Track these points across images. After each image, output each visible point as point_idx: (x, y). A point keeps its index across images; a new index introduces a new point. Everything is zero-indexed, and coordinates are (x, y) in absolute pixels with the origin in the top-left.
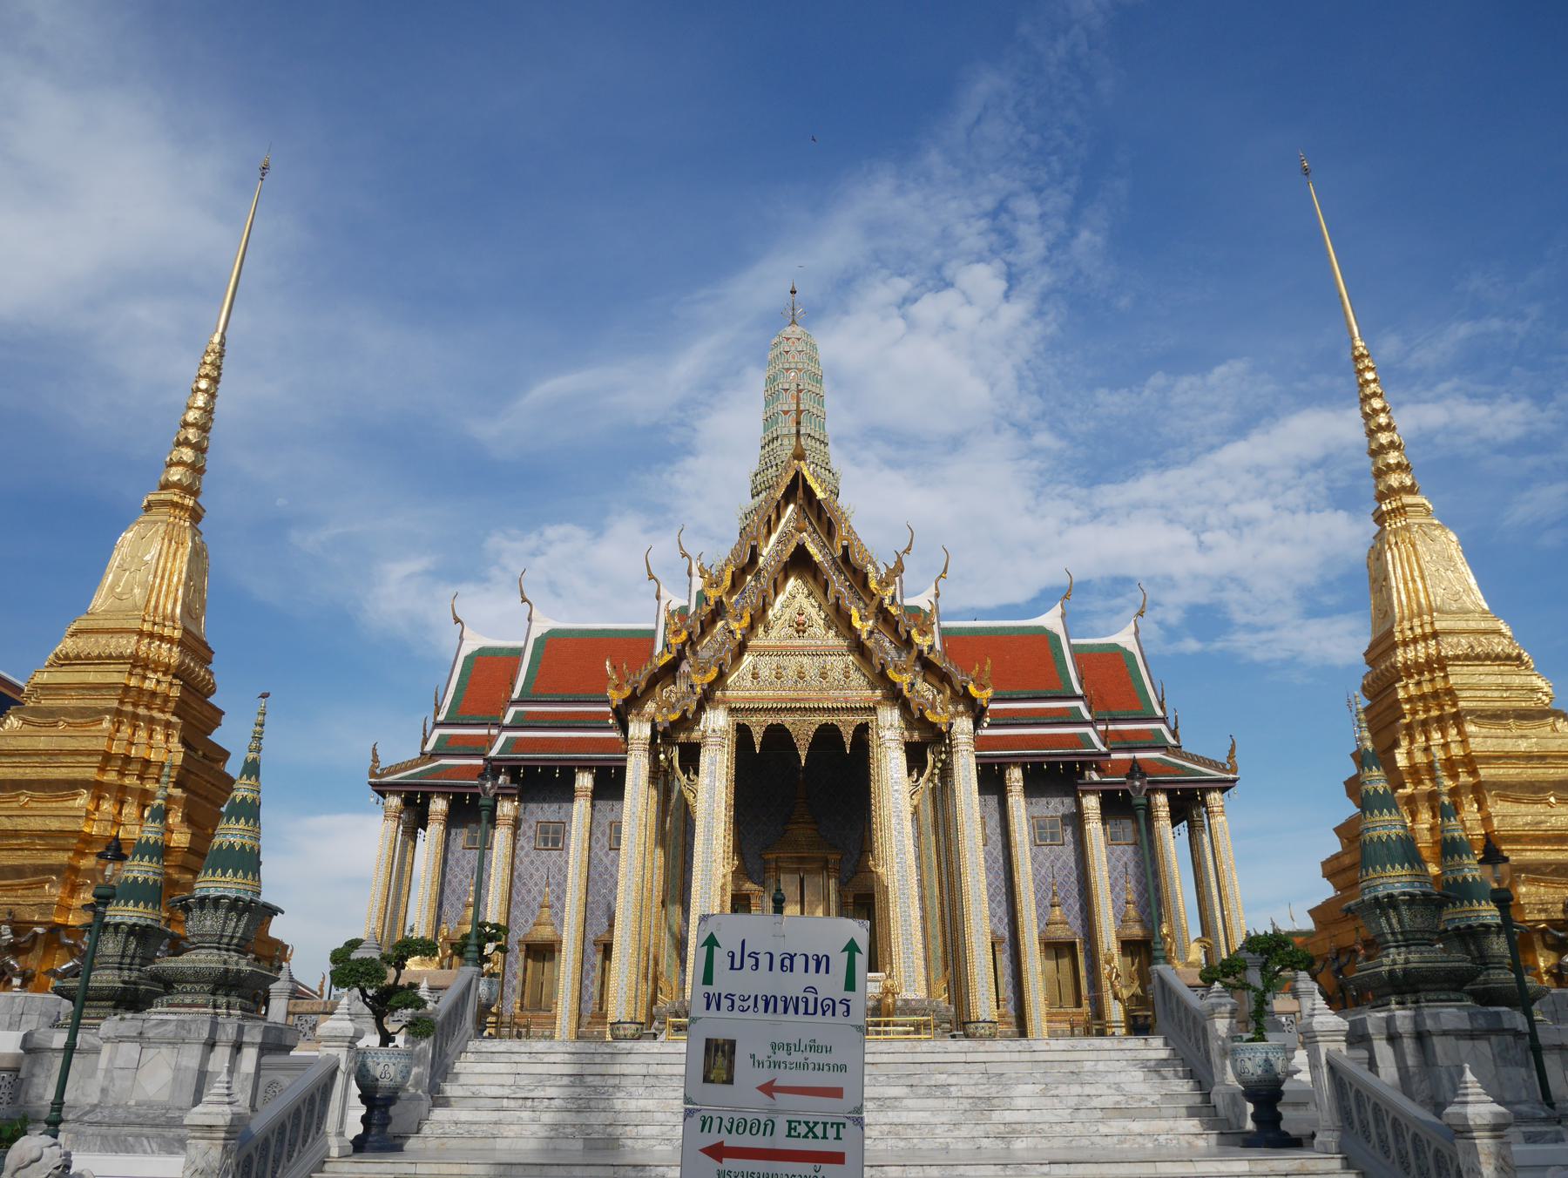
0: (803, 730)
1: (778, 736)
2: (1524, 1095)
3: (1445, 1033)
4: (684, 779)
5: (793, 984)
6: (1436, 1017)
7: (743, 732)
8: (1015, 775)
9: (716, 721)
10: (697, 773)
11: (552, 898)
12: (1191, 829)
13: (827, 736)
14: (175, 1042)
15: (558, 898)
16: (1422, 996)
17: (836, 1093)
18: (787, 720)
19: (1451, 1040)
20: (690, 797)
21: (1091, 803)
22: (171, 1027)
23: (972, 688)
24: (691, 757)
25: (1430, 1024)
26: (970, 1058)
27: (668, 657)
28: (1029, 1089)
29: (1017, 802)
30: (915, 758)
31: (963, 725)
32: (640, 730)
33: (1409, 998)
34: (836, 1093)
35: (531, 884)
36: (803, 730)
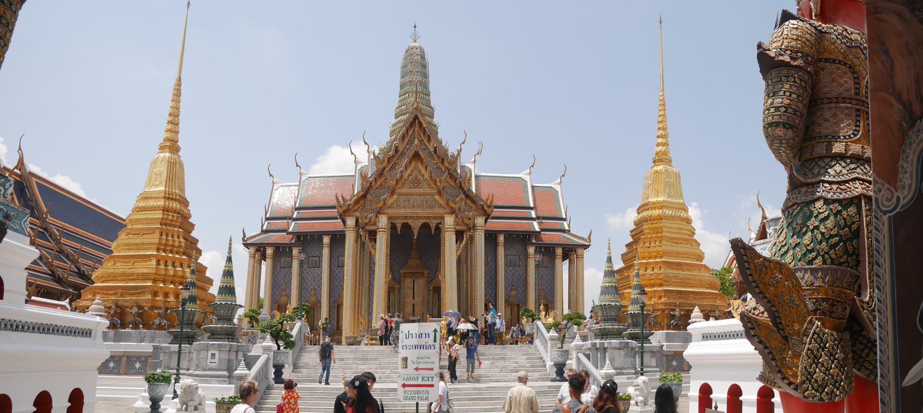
0: (416, 225)
1: (406, 226)
4: (370, 245)
5: (423, 341)
7: (393, 227)
8: (501, 238)
9: (383, 221)
12: (570, 262)
13: (425, 227)
17: (432, 369)
18: (410, 222)
20: (373, 251)
21: (531, 250)
23: (485, 207)
24: (373, 235)
27: (362, 193)
29: (501, 251)
30: (459, 235)
31: (480, 221)
32: (351, 222)
34: (432, 369)
36: (416, 225)
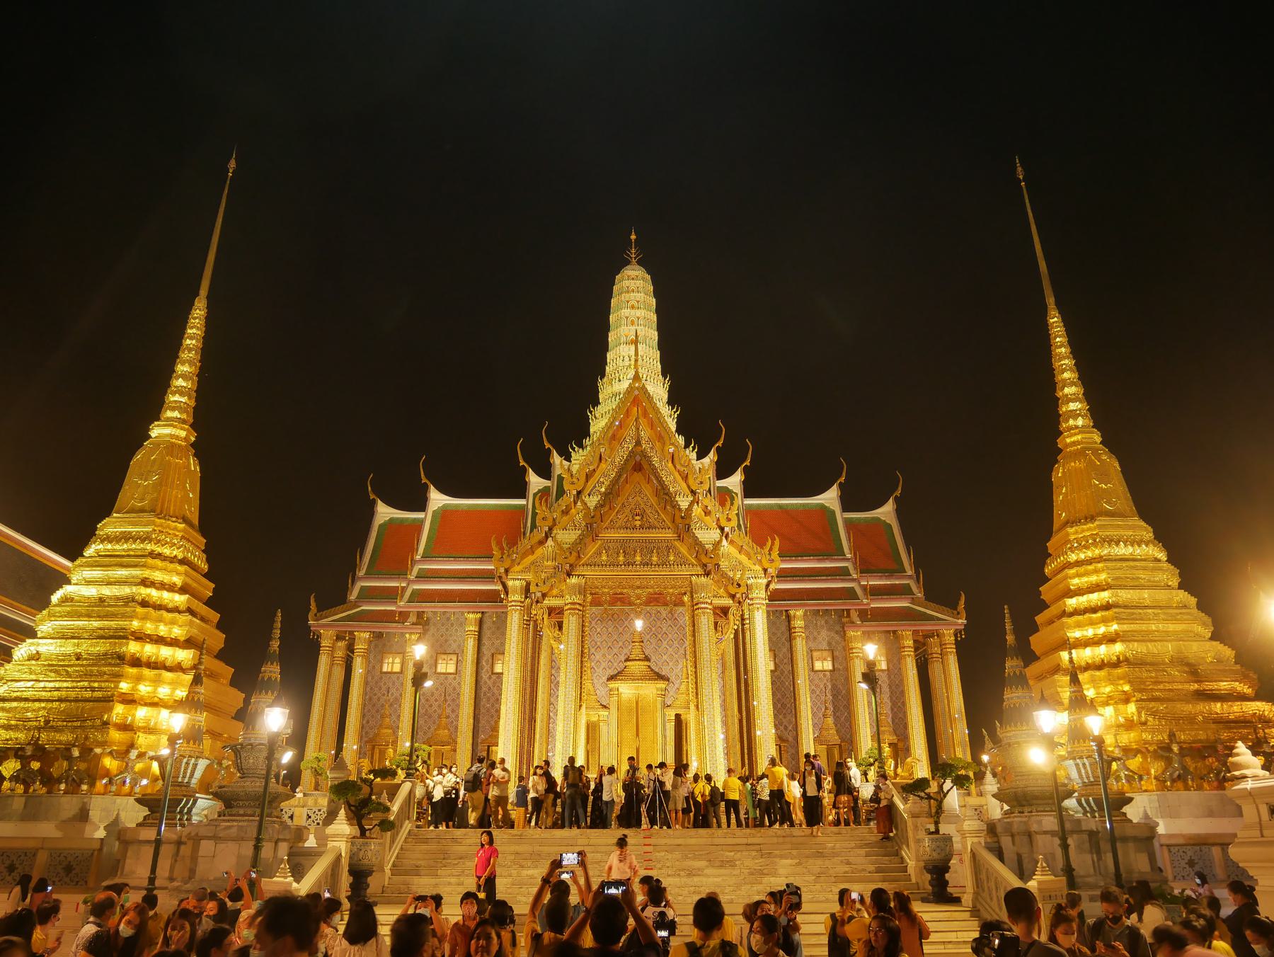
2: (1092, 870)
3: (1046, 833)
6: (1040, 822)
10: (560, 628)
11: (449, 711)
14: (239, 839)
15: (453, 711)
16: (1034, 808)
19: (1048, 836)
20: (555, 645)
22: (234, 830)
25: (1034, 827)
26: (750, 841)
28: (789, 861)
33: (1026, 809)
35: (432, 700)
